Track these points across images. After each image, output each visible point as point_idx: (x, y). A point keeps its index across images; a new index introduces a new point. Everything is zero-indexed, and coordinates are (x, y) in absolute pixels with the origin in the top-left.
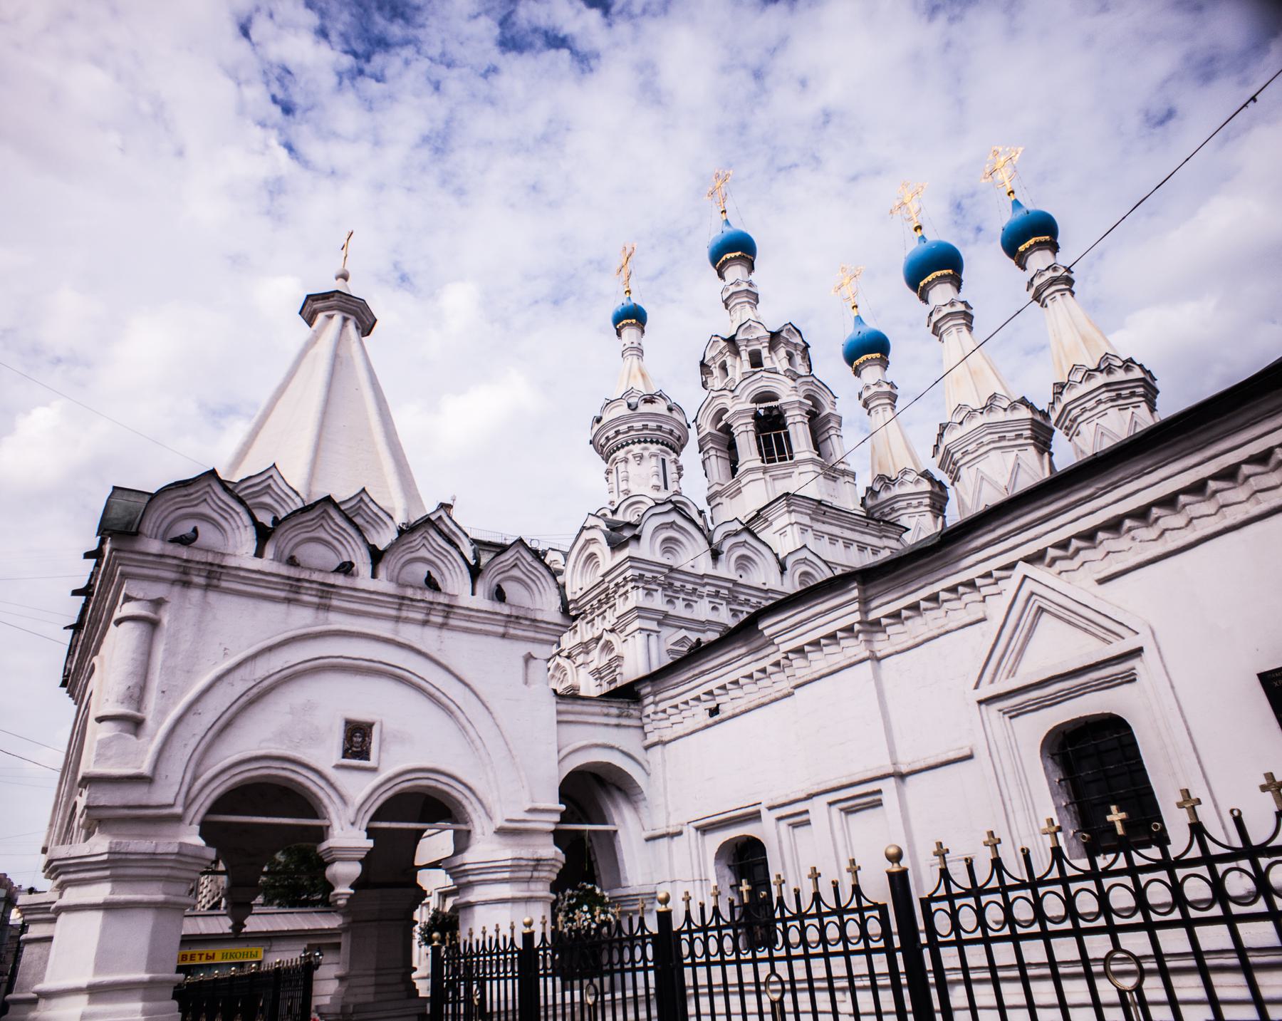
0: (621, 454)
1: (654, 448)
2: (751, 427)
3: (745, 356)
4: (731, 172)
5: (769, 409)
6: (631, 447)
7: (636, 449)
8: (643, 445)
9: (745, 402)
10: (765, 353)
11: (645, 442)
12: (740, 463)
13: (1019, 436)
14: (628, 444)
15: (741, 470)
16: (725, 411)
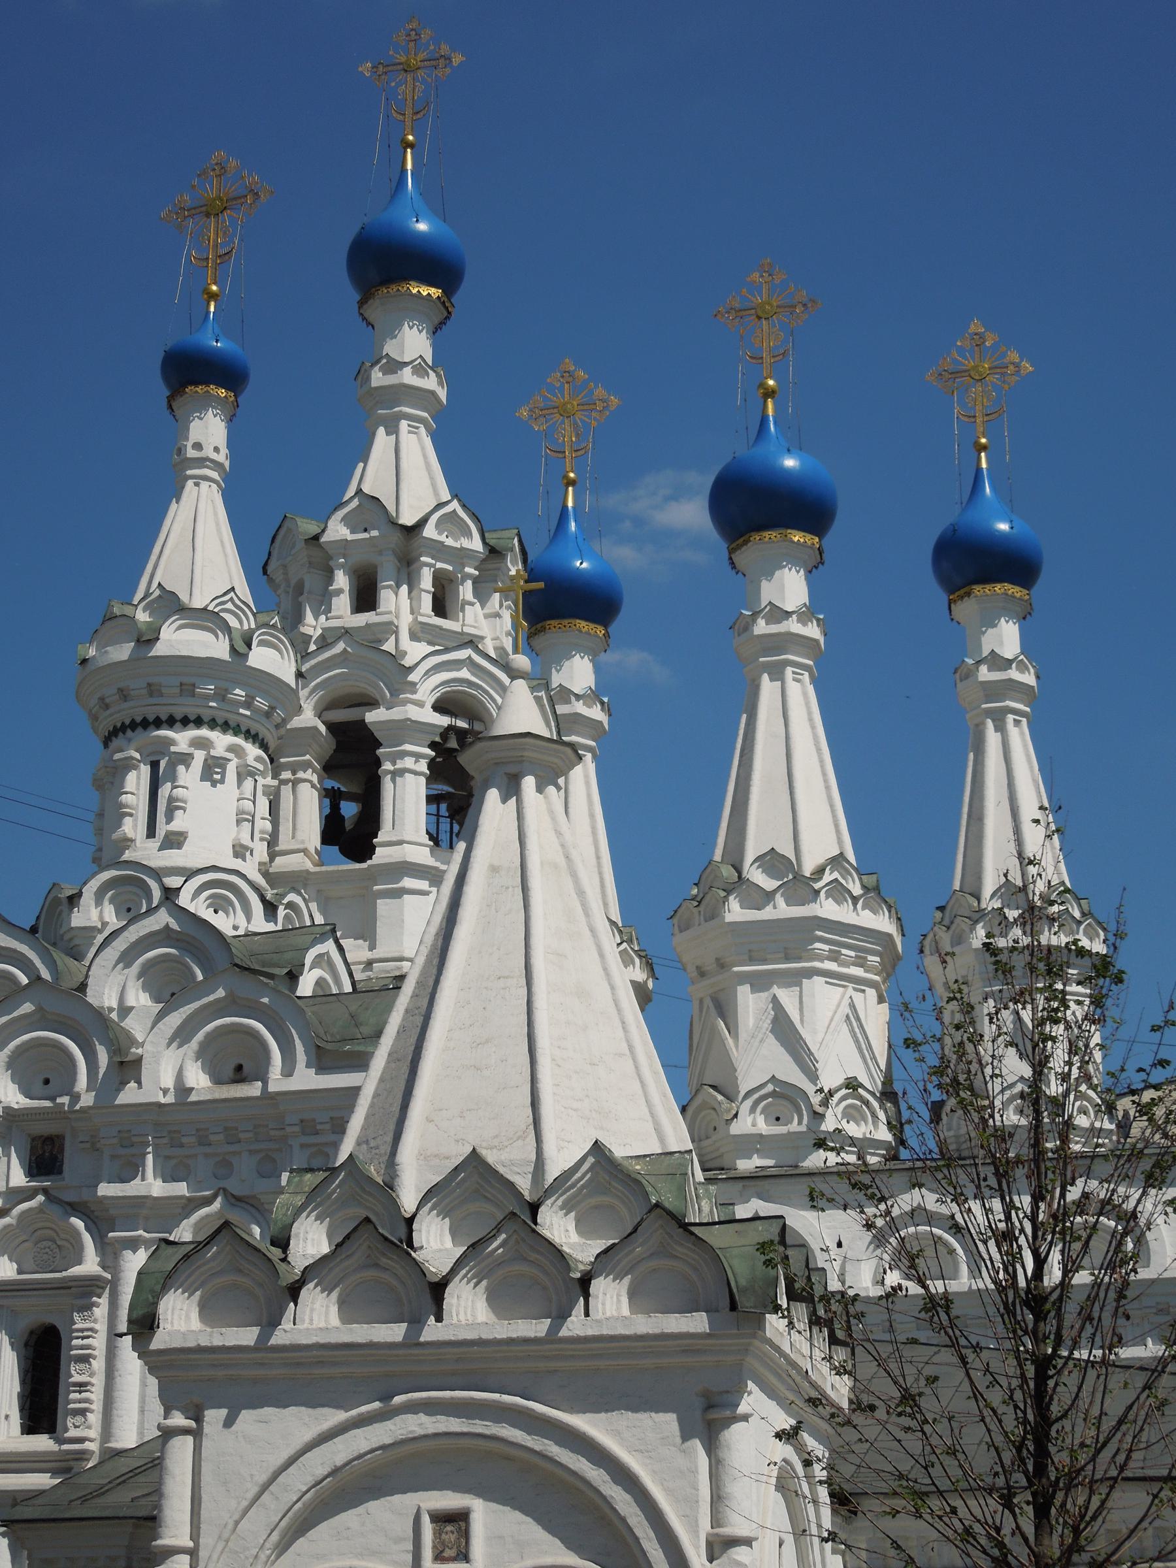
0: (181, 739)
1: (253, 751)
2: (423, 766)
3: (426, 581)
4: (457, 59)
5: (461, 734)
6: (204, 732)
7: (221, 741)
8: (230, 739)
9: (420, 704)
10: (466, 591)
11: (237, 731)
12: (382, 837)
13: (860, 962)
14: (199, 722)
15: (382, 855)
16: (372, 704)
